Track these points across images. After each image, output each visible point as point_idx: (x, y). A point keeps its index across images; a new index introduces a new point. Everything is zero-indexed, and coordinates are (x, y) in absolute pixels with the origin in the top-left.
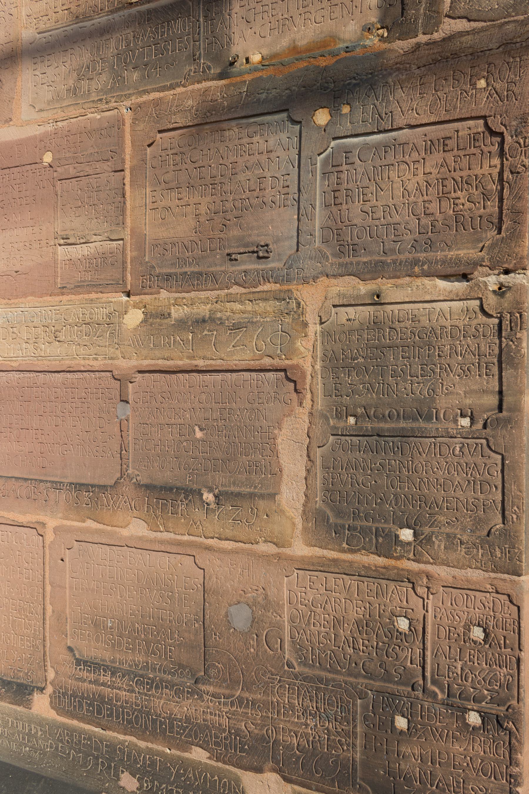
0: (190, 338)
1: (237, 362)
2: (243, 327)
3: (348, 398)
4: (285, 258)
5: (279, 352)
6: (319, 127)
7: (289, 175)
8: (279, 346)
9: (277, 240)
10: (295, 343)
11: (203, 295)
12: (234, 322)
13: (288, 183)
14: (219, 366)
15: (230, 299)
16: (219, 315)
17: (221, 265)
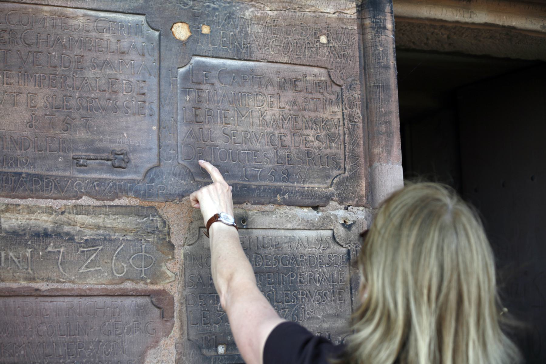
0: (28, 254)
1: (92, 286)
2: (98, 245)
3: (217, 326)
4: (143, 171)
5: (143, 275)
6: (179, 41)
7: (144, 81)
8: (143, 269)
9: (135, 150)
10: (161, 266)
11: (43, 203)
12: (85, 238)
13: (145, 91)
14: (68, 290)
15: (79, 210)
16: (66, 229)
17: (65, 170)
